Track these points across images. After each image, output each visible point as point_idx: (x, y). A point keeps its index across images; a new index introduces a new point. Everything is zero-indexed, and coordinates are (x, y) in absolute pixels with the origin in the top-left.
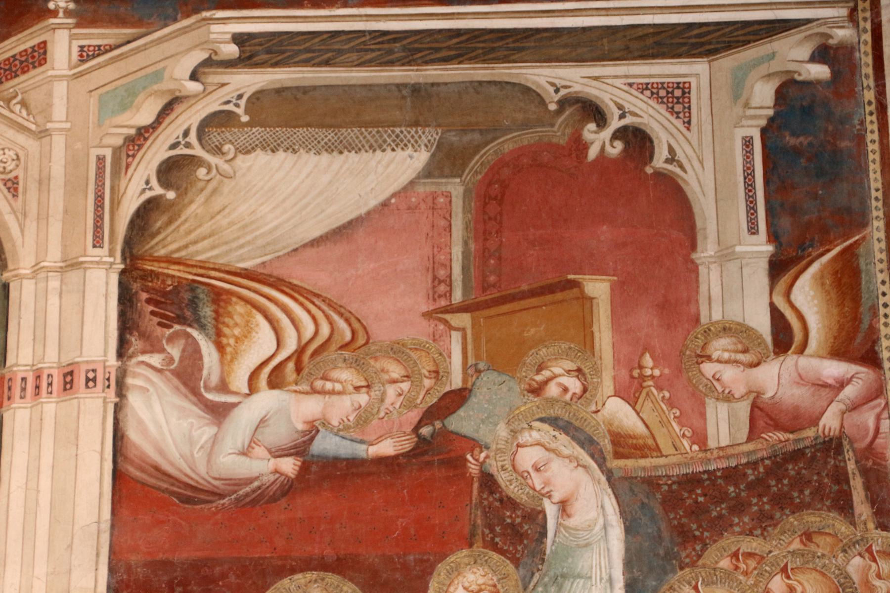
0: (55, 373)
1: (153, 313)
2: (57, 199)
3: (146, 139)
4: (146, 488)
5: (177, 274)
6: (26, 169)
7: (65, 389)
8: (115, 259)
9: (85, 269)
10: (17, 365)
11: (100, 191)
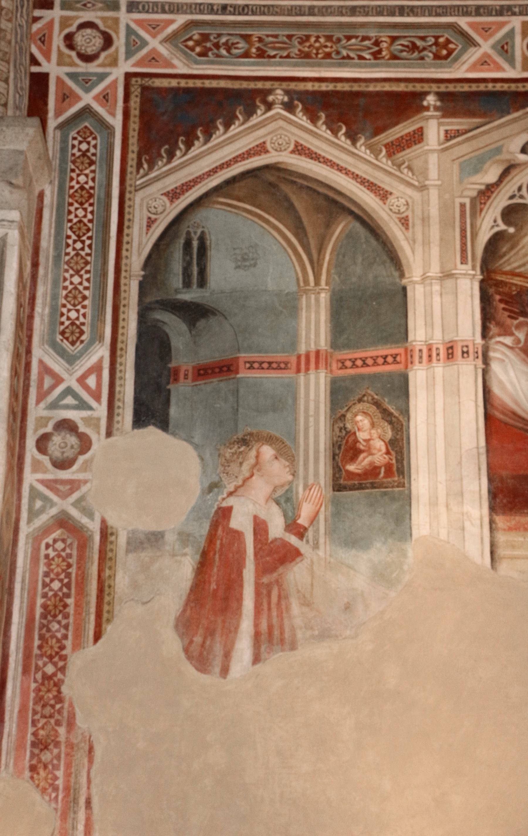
0: (441, 347)
1: (504, 309)
2: (435, 232)
3: (492, 192)
4: (508, 427)
5: (519, 283)
6: (413, 211)
7: (448, 358)
9: (457, 278)
10: (415, 341)
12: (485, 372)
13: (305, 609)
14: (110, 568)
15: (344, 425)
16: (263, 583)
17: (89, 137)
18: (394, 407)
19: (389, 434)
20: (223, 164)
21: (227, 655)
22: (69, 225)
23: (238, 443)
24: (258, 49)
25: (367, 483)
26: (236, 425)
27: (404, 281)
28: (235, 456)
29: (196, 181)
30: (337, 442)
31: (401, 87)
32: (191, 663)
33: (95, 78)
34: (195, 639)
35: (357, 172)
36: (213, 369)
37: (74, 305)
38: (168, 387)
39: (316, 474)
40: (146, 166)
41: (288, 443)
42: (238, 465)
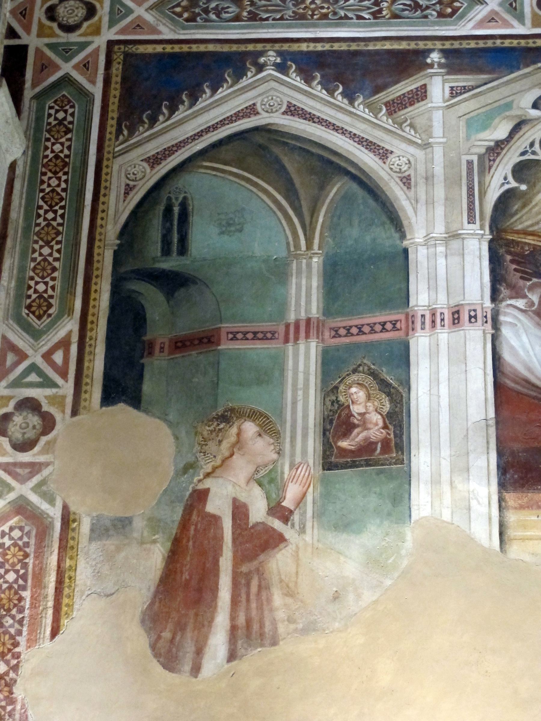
0: (446, 312)
1: (515, 270)
2: (440, 192)
3: (502, 149)
5: (532, 242)
6: (416, 170)
7: (454, 324)
8: (485, 232)
9: (463, 239)
10: (417, 306)
11: (470, 184)
12: (495, 338)
13: (289, 600)
14: (71, 558)
15: (337, 397)
16: (241, 572)
17: (66, 105)
18: (393, 378)
19: (387, 407)
20: (209, 127)
21: (199, 652)
22: (41, 195)
23: (217, 419)
24: (250, 12)
25: (362, 460)
26: (216, 400)
27: (406, 243)
28: (214, 434)
29: (179, 146)
30: (328, 416)
31: (404, 46)
32: (158, 661)
33: (75, 48)
34: (163, 634)
35: (354, 131)
36: (191, 341)
37: (43, 278)
38: (142, 361)
39: (304, 452)
40: (125, 132)
41: (273, 419)
42: (217, 443)
